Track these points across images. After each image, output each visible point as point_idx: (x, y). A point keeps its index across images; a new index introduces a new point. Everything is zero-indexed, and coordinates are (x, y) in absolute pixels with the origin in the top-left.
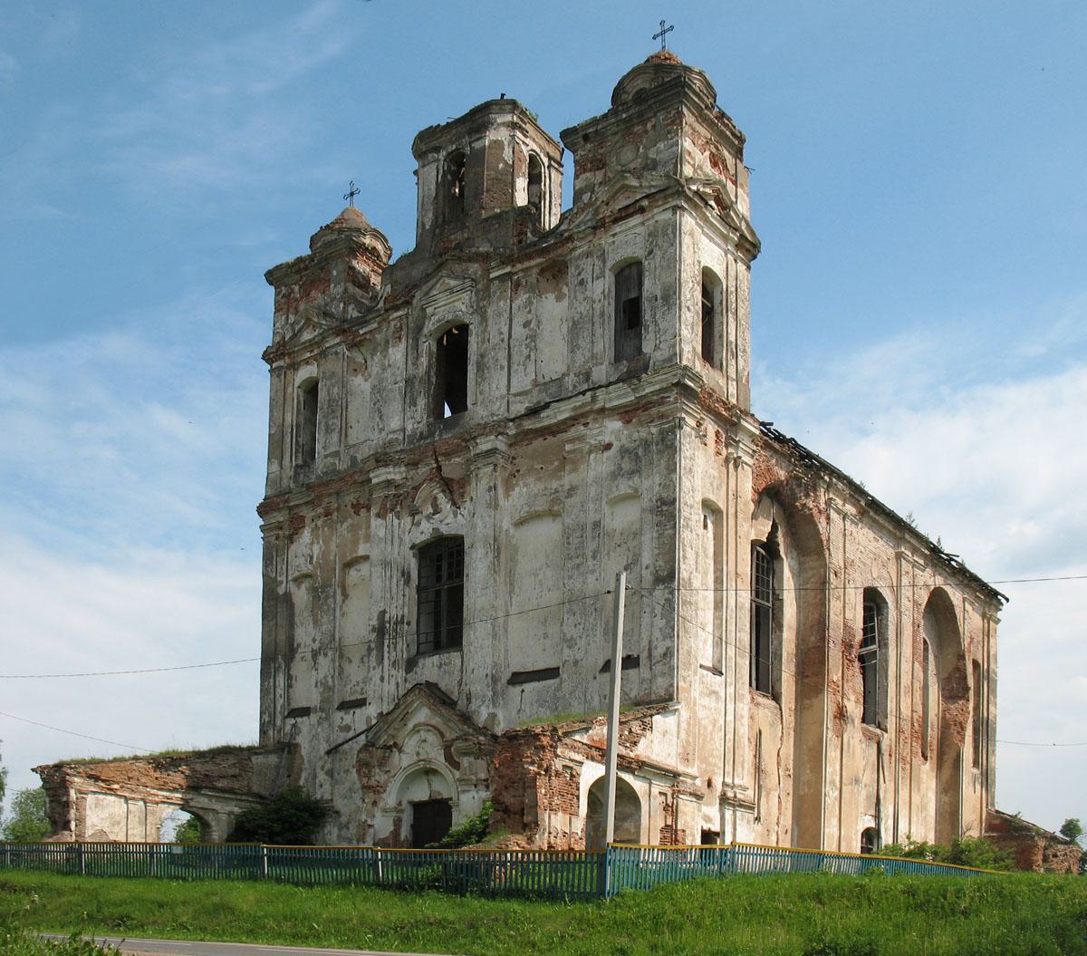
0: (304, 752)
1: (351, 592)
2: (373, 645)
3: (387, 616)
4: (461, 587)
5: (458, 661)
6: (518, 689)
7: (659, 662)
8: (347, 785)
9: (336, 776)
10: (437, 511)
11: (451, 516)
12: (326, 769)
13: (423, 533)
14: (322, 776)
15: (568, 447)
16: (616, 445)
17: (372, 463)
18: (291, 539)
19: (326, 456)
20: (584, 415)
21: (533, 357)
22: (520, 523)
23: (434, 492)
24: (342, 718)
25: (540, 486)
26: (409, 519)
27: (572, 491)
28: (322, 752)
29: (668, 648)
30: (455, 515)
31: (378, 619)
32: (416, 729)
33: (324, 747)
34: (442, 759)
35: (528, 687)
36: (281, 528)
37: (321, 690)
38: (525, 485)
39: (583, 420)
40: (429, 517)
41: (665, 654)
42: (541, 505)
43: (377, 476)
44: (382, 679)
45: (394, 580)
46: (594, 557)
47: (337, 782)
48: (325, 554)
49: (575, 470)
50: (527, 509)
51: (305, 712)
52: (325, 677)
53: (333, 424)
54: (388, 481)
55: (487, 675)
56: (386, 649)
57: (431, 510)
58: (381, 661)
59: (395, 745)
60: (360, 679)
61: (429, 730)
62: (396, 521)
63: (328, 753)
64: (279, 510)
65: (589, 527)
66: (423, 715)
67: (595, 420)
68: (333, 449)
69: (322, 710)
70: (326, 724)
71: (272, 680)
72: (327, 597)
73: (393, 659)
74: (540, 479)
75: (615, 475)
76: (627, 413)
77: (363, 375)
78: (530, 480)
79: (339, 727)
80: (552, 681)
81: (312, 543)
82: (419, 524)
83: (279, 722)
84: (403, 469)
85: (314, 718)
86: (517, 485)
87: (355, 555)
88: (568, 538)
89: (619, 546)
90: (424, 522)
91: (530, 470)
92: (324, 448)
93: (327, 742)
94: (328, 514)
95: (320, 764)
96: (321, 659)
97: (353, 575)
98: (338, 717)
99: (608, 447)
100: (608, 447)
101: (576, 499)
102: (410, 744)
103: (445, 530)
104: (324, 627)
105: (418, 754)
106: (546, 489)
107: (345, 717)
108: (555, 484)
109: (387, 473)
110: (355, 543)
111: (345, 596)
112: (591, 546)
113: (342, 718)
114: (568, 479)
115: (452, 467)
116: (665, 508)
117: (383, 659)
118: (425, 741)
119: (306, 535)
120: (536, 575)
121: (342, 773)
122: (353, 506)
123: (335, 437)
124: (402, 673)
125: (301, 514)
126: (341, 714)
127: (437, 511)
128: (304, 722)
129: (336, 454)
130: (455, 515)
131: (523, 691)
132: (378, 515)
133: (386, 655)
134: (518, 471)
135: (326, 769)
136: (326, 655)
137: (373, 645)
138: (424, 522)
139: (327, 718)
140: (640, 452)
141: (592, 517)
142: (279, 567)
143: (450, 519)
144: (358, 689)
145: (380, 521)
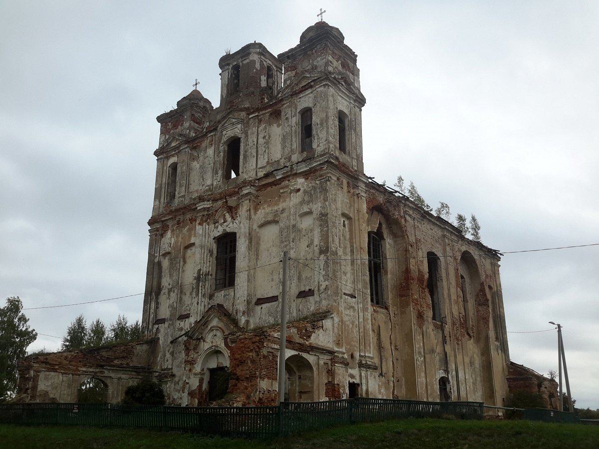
0: (161, 342)
1: (188, 261)
2: (194, 287)
3: (201, 273)
4: (235, 257)
5: (232, 294)
6: (260, 307)
7: (323, 292)
9: (175, 355)
11: (231, 223)
12: (170, 351)
13: (219, 231)
15: (281, 191)
17: (197, 200)
18: (162, 236)
19: (179, 197)
20: (288, 176)
21: (267, 151)
22: (262, 226)
23: (225, 212)
24: (179, 324)
25: (270, 209)
27: (283, 210)
28: (169, 341)
29: (327, 286)
31: (197, 273)
33: (170, 339)
34: (223, 345)
35: (264, 306)
36: (158, 231)
37: (171, 309)
38: (264, 208)
39: (287, 179)
40: (221, 225)
41: (325, 289)
42: (270, 218)
45: (206, 254)
46: (293, 242)
47: (175, 359)
48: (176, 242)
49: (285, 201)
50: (264, 220)
51: (163, 321)
52: (173, 303)
53: (183, 183)
54: (204, 208)
55: (245, 300)
56: (200, 288)
58: (197, 295)
60: (189, 303)
61: (218, 330)
62: (207, 226)
63: (172, 342)
64: (158, 222)
65: (291, 227)
66: (215, 322)
67: (293, 178)
68: (182, 194)
69: (171, 320)
70: (172, 327)
71: (149, 305)
73: (203, 293)
74: (269, 206)
75: (302, 203)
76: (306, 175)
77: (197, 161)
80: (275, 303)
83: (150, 327)
85: (167, 324)
86: (260, 208)
87: (189, 243)
88: (282, 233)
89: (304, 236)
90: (219, 227)
91: (265, 202)
93: (172, 336)
95: (168, 349)
96: (172, 294)
97: (189, 252)
99: (299, 190)
100: (299, 190)
101: (285, 215)
102: (209, 338)
103: (228, 230)
105: (212, 342)
106: (272, 210)
108: (276, 208)
109: (204, 204)
110: (190, 237)
111: (185, 262)
112: (292, 236)
113: (179, 324)
114: (282, 205)
115: (232, 202)
116: (323, 218)
117: (198, 293)
118: (216, 335)
119: (169, 234)
120: (268, 251)
121: (178, 354)
122: (190, 220)
123: (183, 189)
124: (207, 300)
125: (167, 224)
128: (162, 327)
129: (184, 196)
131: (262, 308)
132: (199, 224)
133: (200, 291)
134: (260, 202)
135: (170, 351)
136: (174, 292)
137: (194, 287)
138: (219, 227)
140: (312, 192)
141: (292, 222)
142: (156, 249)
145: (200, 227)
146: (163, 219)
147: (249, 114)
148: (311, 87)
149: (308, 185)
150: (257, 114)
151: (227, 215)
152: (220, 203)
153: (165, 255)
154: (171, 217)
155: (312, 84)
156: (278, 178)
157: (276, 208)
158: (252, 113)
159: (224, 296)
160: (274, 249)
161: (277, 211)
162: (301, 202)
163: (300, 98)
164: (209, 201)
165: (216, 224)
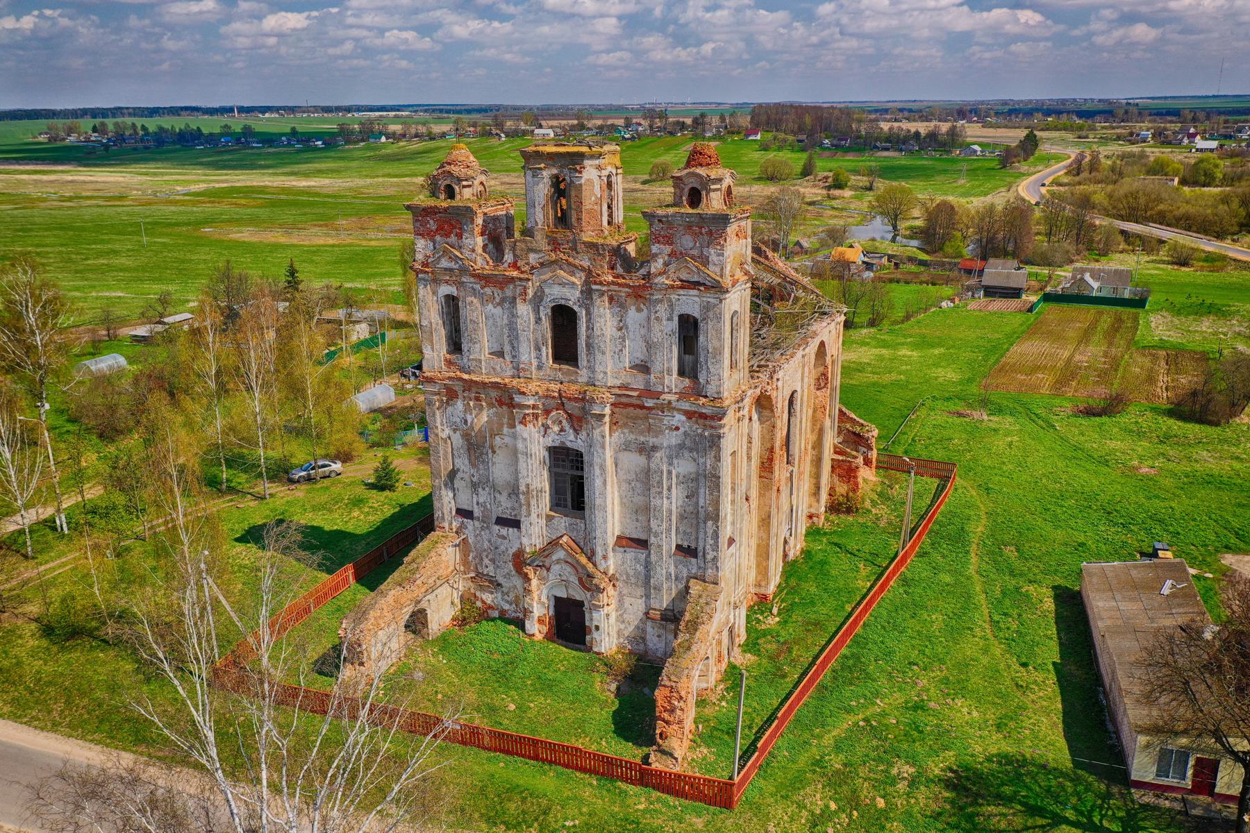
3: (531, 487)
8: (506, 571)
14: (486, 561)
16: (682, 430)
32: (558, 561)
38: (624, 433)
47: (498, 567)
49: (657, 437)
59: (544, 566)
70: (487, 531)
72: (482, 454)
78: (626, 431)
81: (465, 411)
91: (625, 425)
94: (478, 399)
95: (485, 554)
99: (677, 429)
100: (677, 429)
103: (569, 445)
119: (460, 404)
126: (497, 527)
139: (488, 528)
143: (572, 437)
149: (691, 427)
157: (642, 439)
160: (638, 485)
161: (643, 443)
162: (679, 445)
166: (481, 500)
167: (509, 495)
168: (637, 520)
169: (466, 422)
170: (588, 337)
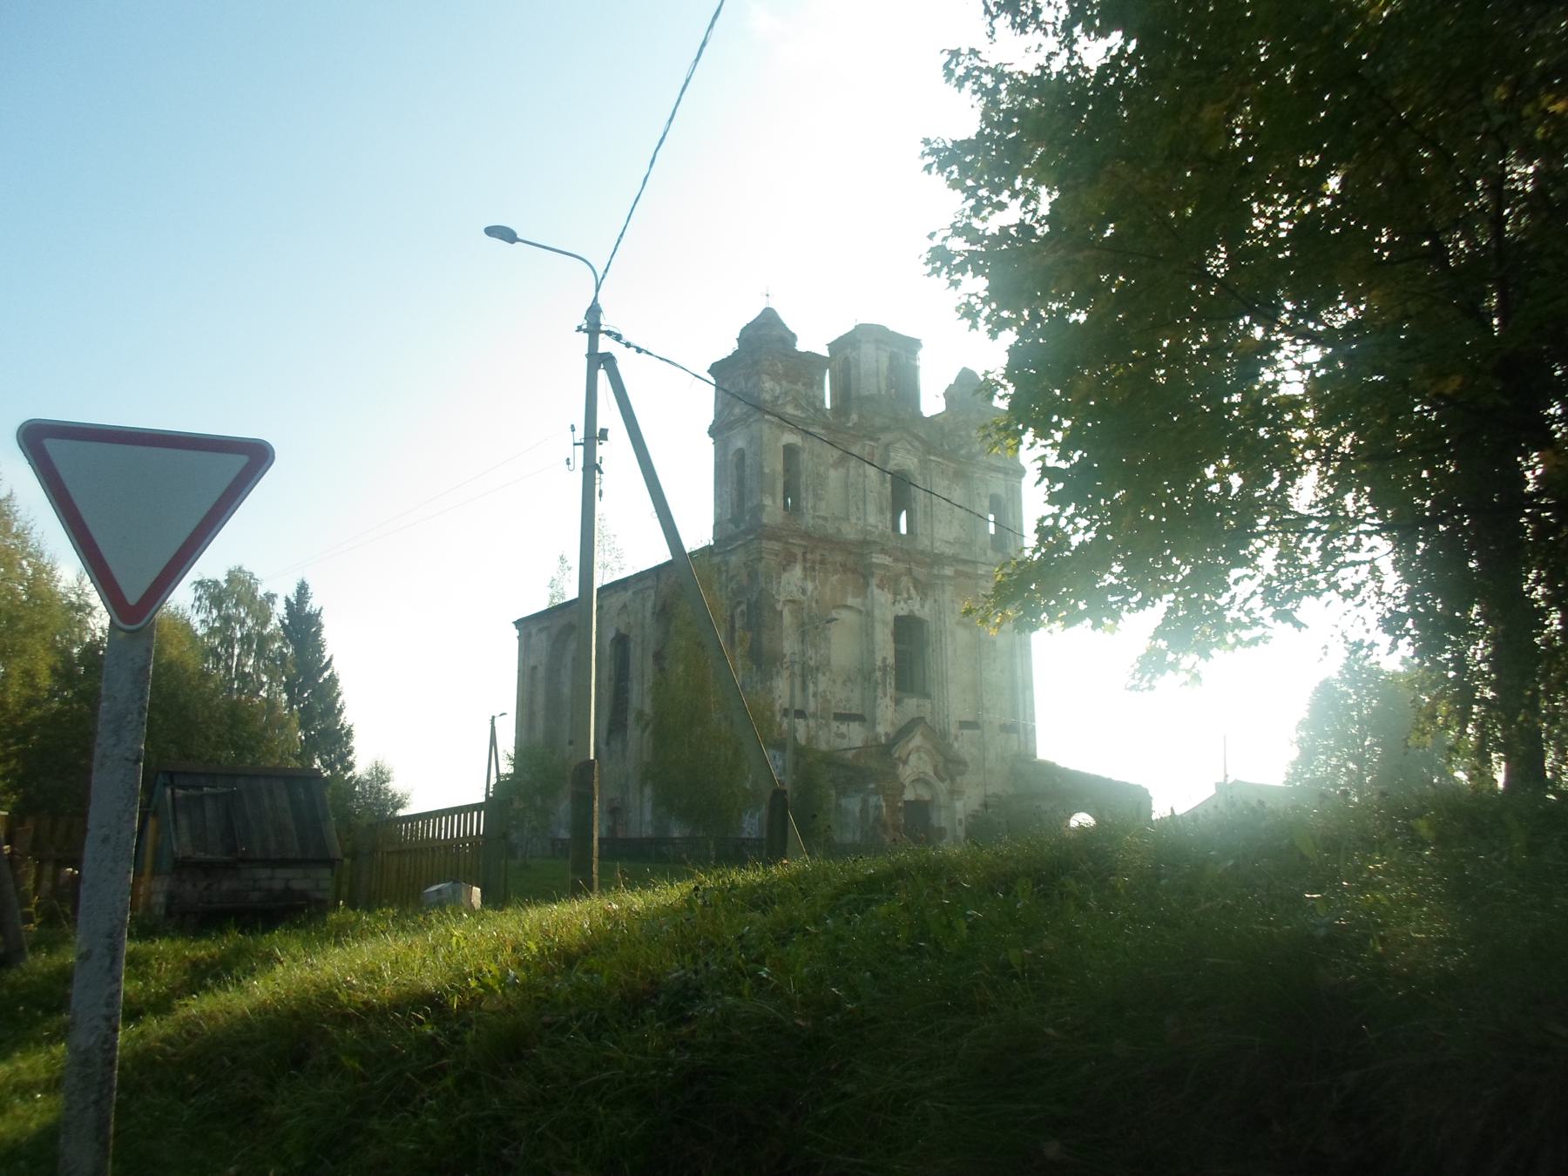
5: (929, 706)
10: (910, 598)
13: (902, 609)
19: (819, 517)
24: (838, 727)
26: (890, 597)
30: (922, 606)
32: (918, 749)
34: (932, 773)
43: (877, 558)
44: (887, 707)
52: (825, 692)
57: (905, 595)
68: (822, 513)
79: (836, 733)
81: (805, 578)
82: (899, 602)
84: (891, 560)
92: (814, 508)
94: (822, 562)
98: (834, 724)
102: (913, 759)
104: (822, 652)
107: (841, 727)
113: (838, 727)
119: (798, 571)
122: (841, 565)
127: (910, 598)
130: (922, 606)
132: (878, 586)
136: (824, 674)
138: (902, 602)
139: (827, 725)
143: (917, 606)
144: (842, 705)
145: (879, 591)
146: (790, 541)
147: (929, 453)
148: (1007, 474)
150: (940, 460)
151: (913, 591)
152: (901, 566)
153: (784, 604)
154: (804, 543)
155: (1011, 472)
156: (979, 572)
158: (935, 455)
159: (918, 706)
163: (992, 477)
164: (890, 556)
165: (898, 597)
166: (821, 689)
167: (844, 683)
168: (965, 700)
169: (804, 592)
170: (925, 506)
